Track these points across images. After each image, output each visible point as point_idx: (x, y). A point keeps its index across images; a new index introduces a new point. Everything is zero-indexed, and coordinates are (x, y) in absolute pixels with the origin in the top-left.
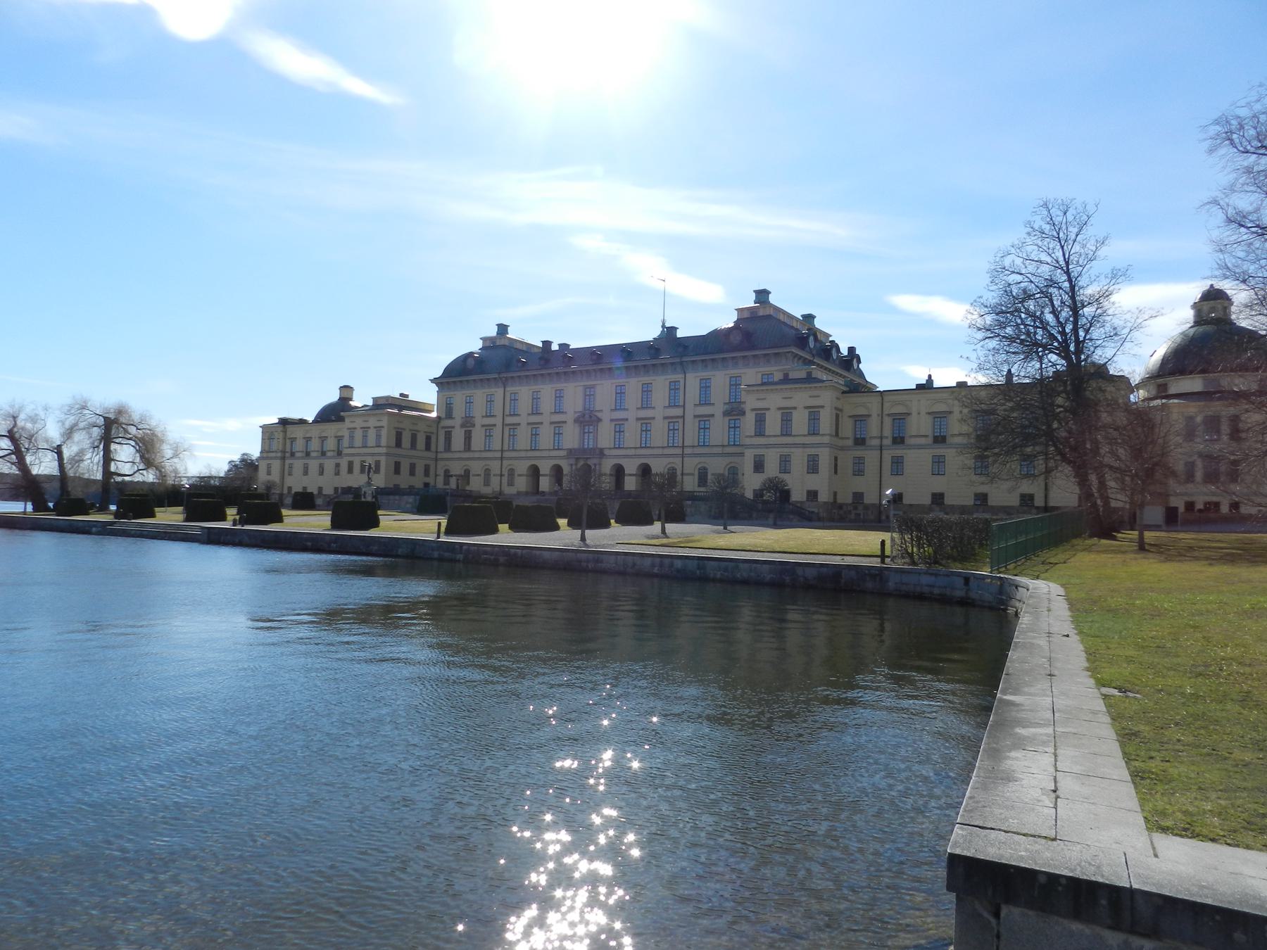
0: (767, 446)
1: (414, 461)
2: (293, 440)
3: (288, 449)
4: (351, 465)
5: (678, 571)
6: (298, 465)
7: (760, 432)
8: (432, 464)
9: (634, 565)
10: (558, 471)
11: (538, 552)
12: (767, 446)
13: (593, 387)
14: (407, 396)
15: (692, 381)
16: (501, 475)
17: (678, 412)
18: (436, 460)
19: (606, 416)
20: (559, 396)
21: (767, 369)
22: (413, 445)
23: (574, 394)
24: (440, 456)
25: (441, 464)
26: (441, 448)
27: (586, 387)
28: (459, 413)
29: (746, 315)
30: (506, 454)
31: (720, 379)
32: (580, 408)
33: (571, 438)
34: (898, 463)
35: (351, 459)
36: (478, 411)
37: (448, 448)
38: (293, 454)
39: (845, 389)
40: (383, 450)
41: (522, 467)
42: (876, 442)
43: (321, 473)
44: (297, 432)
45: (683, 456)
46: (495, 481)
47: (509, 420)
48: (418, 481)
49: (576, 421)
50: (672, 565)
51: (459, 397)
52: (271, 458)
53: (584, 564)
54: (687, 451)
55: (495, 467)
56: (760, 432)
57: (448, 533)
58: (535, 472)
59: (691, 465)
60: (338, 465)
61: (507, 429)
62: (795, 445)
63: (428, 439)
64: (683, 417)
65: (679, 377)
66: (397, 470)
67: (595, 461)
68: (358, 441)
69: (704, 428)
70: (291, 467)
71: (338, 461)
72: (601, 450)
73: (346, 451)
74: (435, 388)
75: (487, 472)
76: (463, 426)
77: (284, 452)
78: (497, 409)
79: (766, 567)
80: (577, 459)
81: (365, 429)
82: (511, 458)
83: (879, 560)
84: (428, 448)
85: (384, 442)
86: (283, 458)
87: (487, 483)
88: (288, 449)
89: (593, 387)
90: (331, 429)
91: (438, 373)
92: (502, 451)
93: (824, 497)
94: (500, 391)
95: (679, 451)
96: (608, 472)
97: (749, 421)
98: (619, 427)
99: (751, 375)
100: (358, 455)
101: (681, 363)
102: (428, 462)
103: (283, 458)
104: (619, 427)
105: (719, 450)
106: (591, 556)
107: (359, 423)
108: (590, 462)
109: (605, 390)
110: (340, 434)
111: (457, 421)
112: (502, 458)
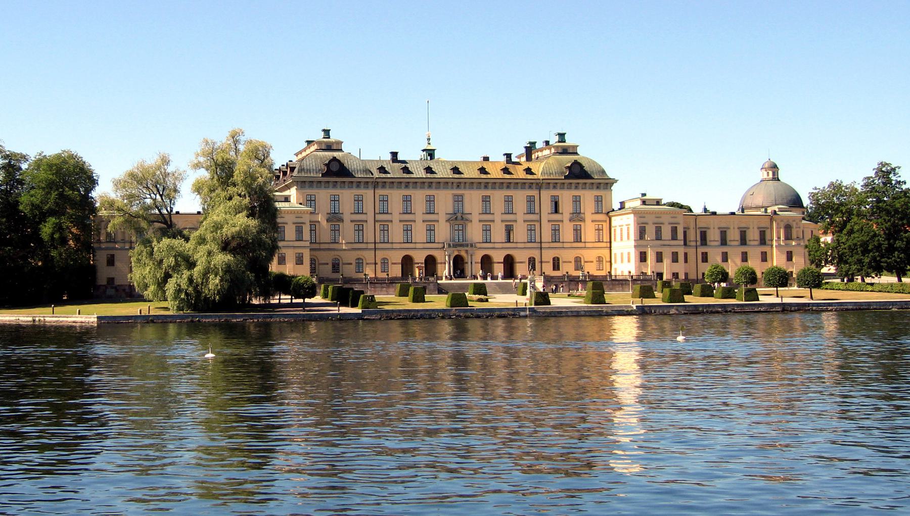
10: (431, 263)
13: (462, 196)
15: (546, 196)
16: (376, 264)
19: (475, 217)
20: (430, 200)
23: (444, 200)
27: (455, 195)
30: (378, 246)
31: (566, 197)
34: (705, 258)
41: (397, 257)
42: (693, 244)
47: (379, 217)
51: (323, 196)
54: (544, 245)
55: (368, 256)
58: (407, 262)
59: (548, 255)
61: (377, 224)
65: (534, 192)
78: (368, 206)
89: (462, 196)
93: (682, 277)
99: (588, 197)
108: (463, 254)
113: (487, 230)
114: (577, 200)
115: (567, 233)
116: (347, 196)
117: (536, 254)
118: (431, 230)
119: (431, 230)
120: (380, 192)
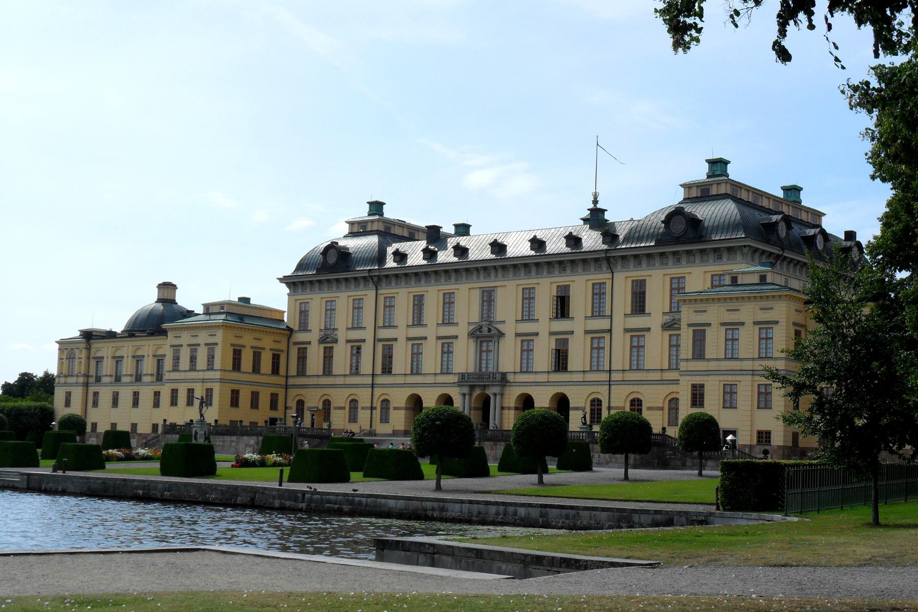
0: (708, 373)
1: (255, 389)
2: (99, 360)
3: (92, 372)
4: (174, 392)
5: (522, 519)
6: (105, 395)
7: (699, 353)
8: (281, 392)
9: (479, 513)
11: (383, 501)
12: (708, 373)
14: (246, 300)
17: (603, 324)
18: (287, 387)
19: (509, 329)
20: (448, 302)
21: (718, 268)
22: (256, 369)
23: (467, 298)
24: (291, 381)
25: (292, 393)
26: (293, 371)
28: (316, 322)
29: (695, 193)
31: (657, 282)
32: (475, 317)
33: (465, 358)
35: (174, 386)
36: (342, 320)
37: (302, 372)
38: (98, 379)
39: (806, 298)
40: (217, 375)
41: (399, 398)
43: (136, 403)
44: (104, 349)
45: (610, 383)
46: (363, 416)
47: (384, 334)
48: (261, 416)
49: (471, 335)
50: (515, 513)
51: (316, 301)
52: (71, 385)
53: (429, 513)
54: (616, 377)
55: (364, 397)
56: (699, 353)
57: (291, 480)
60: (157, 394)
62: (742, 372)
63: (276, 358)
64: (610, 331)
65: (603, 276)
66: (235, 402)
67: (496, 390)
68: (184, 363)
69: (637, 348)
70: (96, 394)
71: (157, 388)
72: (504, 375)
73: (167, 376)
74: (285, 290)
75: (354, 403)
76: (322, 341)
77: (87, 376)
79: (604, 514)
80: (472, 387)
81: (194, 347)
82: (383, 386)
83: (715, 507)
84: (275, 370)
85: (217, 364)
86: (86, 385)
87: (353, 418)
88: (92, 372)
90: (148, 347)
91: (289, 270)
92: (373, 375)
94: (371, 293)
95: (604, 377)
96: (512, 405)
97: (686, 337)
98: (527, 341)
99: (698, 277)
100: (185, 381)
101: (608, 259)
102: (274, 390)
103: (86, 385)
104: (527, 341)
105: (656, 376)
106: (436, 505)
107: (186, 339)
109: (507, 294)
110: (160, 352)
111: (313, 336)
112: (373, 386)
113: (527, 351)
114: (677, 286)
115: (656, 349)
116: (343, 299)
117: (602, 393)
118: (447, 351)
119: (447, 351)
120: (384, 291)
